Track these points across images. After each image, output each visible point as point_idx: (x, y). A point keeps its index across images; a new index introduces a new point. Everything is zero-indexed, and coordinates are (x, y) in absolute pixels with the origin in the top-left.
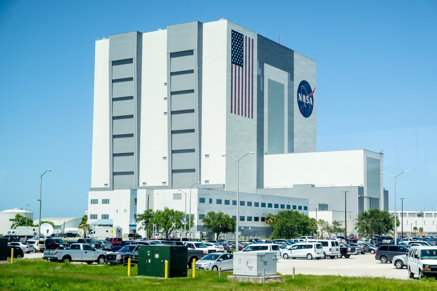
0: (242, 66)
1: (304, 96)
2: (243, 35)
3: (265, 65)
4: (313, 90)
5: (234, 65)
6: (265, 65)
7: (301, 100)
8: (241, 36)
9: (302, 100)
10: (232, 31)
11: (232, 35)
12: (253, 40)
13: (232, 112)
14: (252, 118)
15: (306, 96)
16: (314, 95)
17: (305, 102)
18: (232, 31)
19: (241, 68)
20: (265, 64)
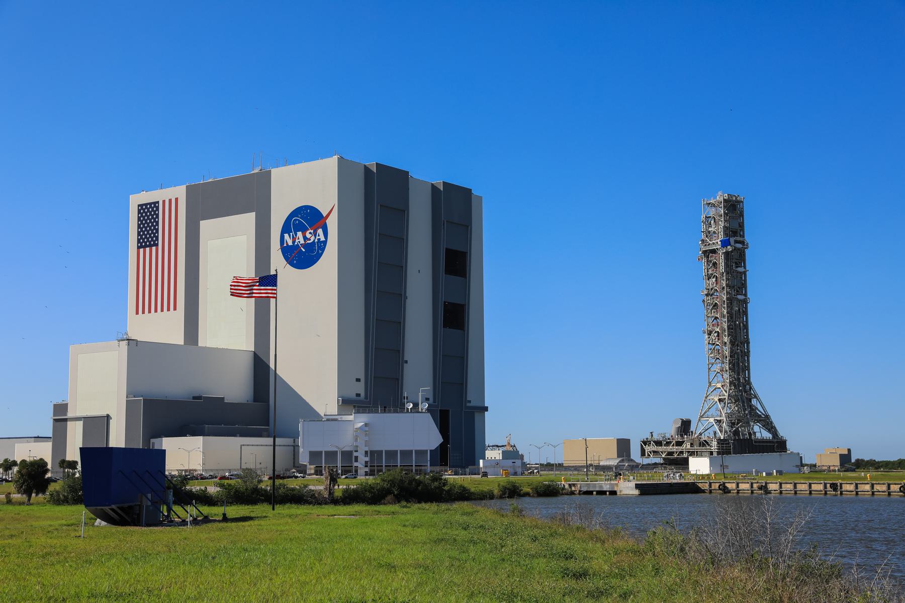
0: (157, 245)
1: (300, 234)
2: (158, 202)
3: (203, 223)
5: (142, 250)
6: (203, 223)
7: (290, 243)
8: (155, 206)
9: (294, 242)
12: (177, 199)
13: (137, 313)
14: (175, 309)
17: (302, 242)
19: (154, 248)
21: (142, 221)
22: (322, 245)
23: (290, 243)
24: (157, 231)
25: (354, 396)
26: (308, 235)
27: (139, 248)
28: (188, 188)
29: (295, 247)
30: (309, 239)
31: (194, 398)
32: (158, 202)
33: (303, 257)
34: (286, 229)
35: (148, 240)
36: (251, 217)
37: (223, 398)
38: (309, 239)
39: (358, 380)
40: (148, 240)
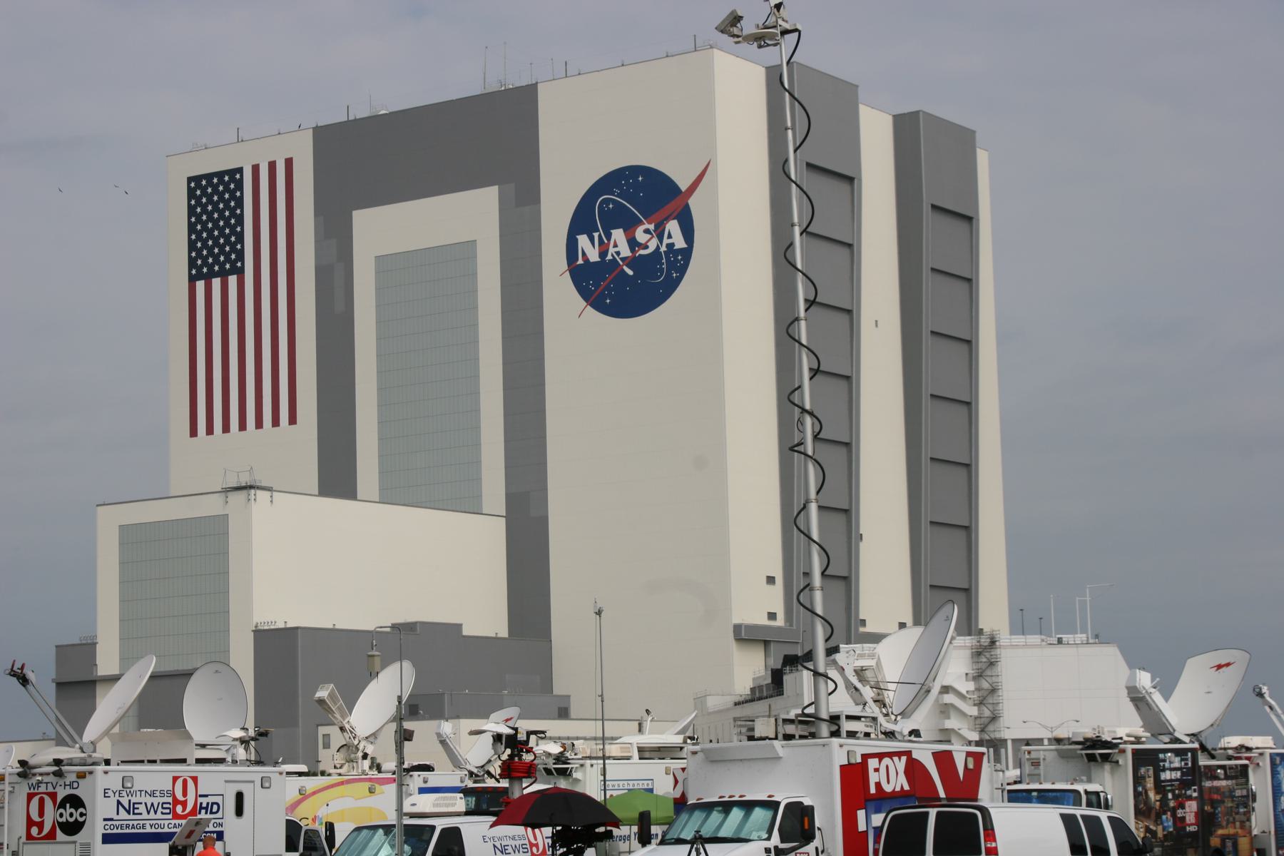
0: (240, 272)
1: (618, 235)
2: (240, 170)
3: (361, 218)
4: (683, 188)
6: (361, 218)
7: (594, 256)
8: (232, 179)
9: (603, 254)
10: (190, 180)
11: (191, 194)
12: (289, 162)
13: (194, 432)
14: (293, 420)
15: (629, 226)
16: (691, 202)
17: (625, 251)
18: (190, 180)
20: (355, 213)
21: (199, 217)
22: (679, 261)
23: (594, 256)
24: (240, 237)
25: (763, 621)
26: (641, 236)
27: (192, 280)
28: (324, 136)
29: (606, 266)
30: (646, 247)
31: (394, 626)
32: (240, 170)
33: (629, 289)
34: (582, 222)
35: (216, 261)
36: (490, 196)
37: (458, 627)
38: (646, 247)
39: (771, 580)
40: (216, 257)
